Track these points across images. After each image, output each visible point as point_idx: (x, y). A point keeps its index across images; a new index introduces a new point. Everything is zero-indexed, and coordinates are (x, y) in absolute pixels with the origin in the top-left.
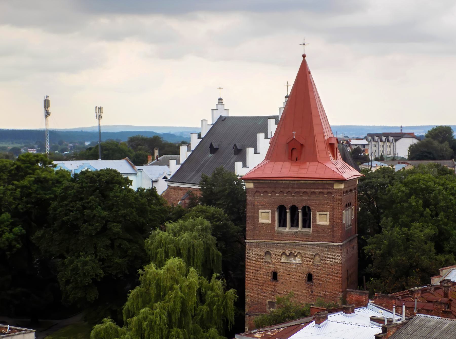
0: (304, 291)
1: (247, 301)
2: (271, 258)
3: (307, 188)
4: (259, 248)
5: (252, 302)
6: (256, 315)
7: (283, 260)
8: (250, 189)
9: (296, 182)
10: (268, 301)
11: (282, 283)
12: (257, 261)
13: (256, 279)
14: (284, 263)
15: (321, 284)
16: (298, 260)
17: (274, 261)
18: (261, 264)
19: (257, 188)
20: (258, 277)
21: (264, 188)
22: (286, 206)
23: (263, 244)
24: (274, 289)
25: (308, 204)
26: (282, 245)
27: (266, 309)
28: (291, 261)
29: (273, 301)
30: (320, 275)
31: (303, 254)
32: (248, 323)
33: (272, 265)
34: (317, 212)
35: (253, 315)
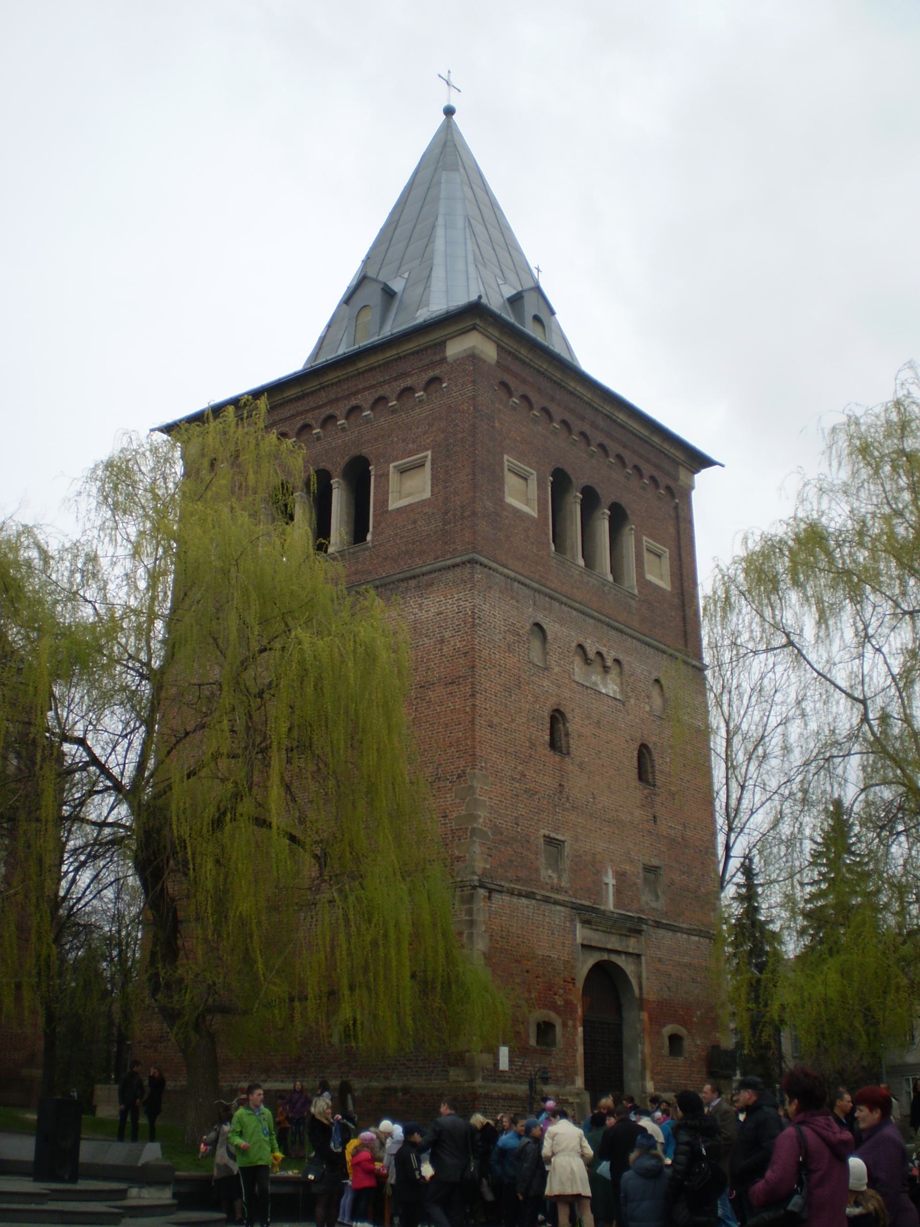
0: (638, 812)
1: (481, 820)
2: (545, 653)
3: (625, 446)
4: (512, 598)
5: (497, 830)
6: (511, 893)
7: (578, 670)
8: (484, 361)
9: (607, 409)
10: (544, 836)
11: (581, 766)
12: (510, 652)
13: (505, 725)
14: (583, 685)
15: (674, 794)
16: (611, 687)
17: (557, 670)
18: (519, 669)
19: (507, 370)
20: (513, 720)
21: (524, 381)
22: (574, 479)
23: (523, 587)
24: (560, 785)
25: (625, 500)
26: (574, 613)
27: (537, 870)
28: (595, 684)
29: (559, 837)
30: (668, 760)
31: (626, 666)
32: (483, 929)
33: (552, 683)
34: (645, 538)
35: (501, 892)
